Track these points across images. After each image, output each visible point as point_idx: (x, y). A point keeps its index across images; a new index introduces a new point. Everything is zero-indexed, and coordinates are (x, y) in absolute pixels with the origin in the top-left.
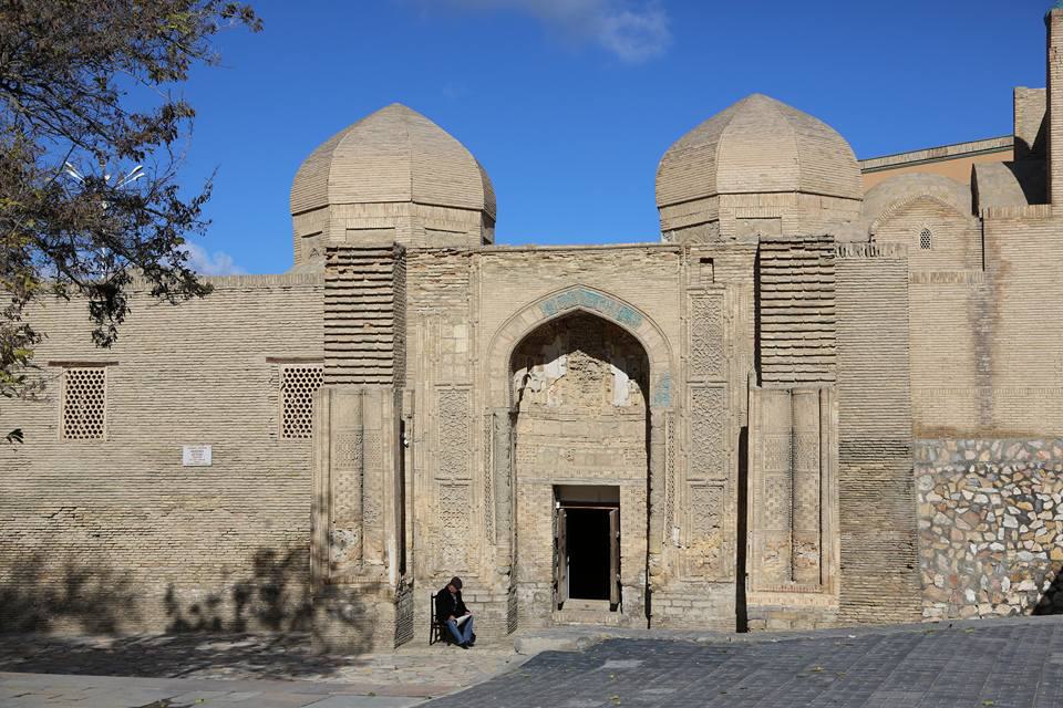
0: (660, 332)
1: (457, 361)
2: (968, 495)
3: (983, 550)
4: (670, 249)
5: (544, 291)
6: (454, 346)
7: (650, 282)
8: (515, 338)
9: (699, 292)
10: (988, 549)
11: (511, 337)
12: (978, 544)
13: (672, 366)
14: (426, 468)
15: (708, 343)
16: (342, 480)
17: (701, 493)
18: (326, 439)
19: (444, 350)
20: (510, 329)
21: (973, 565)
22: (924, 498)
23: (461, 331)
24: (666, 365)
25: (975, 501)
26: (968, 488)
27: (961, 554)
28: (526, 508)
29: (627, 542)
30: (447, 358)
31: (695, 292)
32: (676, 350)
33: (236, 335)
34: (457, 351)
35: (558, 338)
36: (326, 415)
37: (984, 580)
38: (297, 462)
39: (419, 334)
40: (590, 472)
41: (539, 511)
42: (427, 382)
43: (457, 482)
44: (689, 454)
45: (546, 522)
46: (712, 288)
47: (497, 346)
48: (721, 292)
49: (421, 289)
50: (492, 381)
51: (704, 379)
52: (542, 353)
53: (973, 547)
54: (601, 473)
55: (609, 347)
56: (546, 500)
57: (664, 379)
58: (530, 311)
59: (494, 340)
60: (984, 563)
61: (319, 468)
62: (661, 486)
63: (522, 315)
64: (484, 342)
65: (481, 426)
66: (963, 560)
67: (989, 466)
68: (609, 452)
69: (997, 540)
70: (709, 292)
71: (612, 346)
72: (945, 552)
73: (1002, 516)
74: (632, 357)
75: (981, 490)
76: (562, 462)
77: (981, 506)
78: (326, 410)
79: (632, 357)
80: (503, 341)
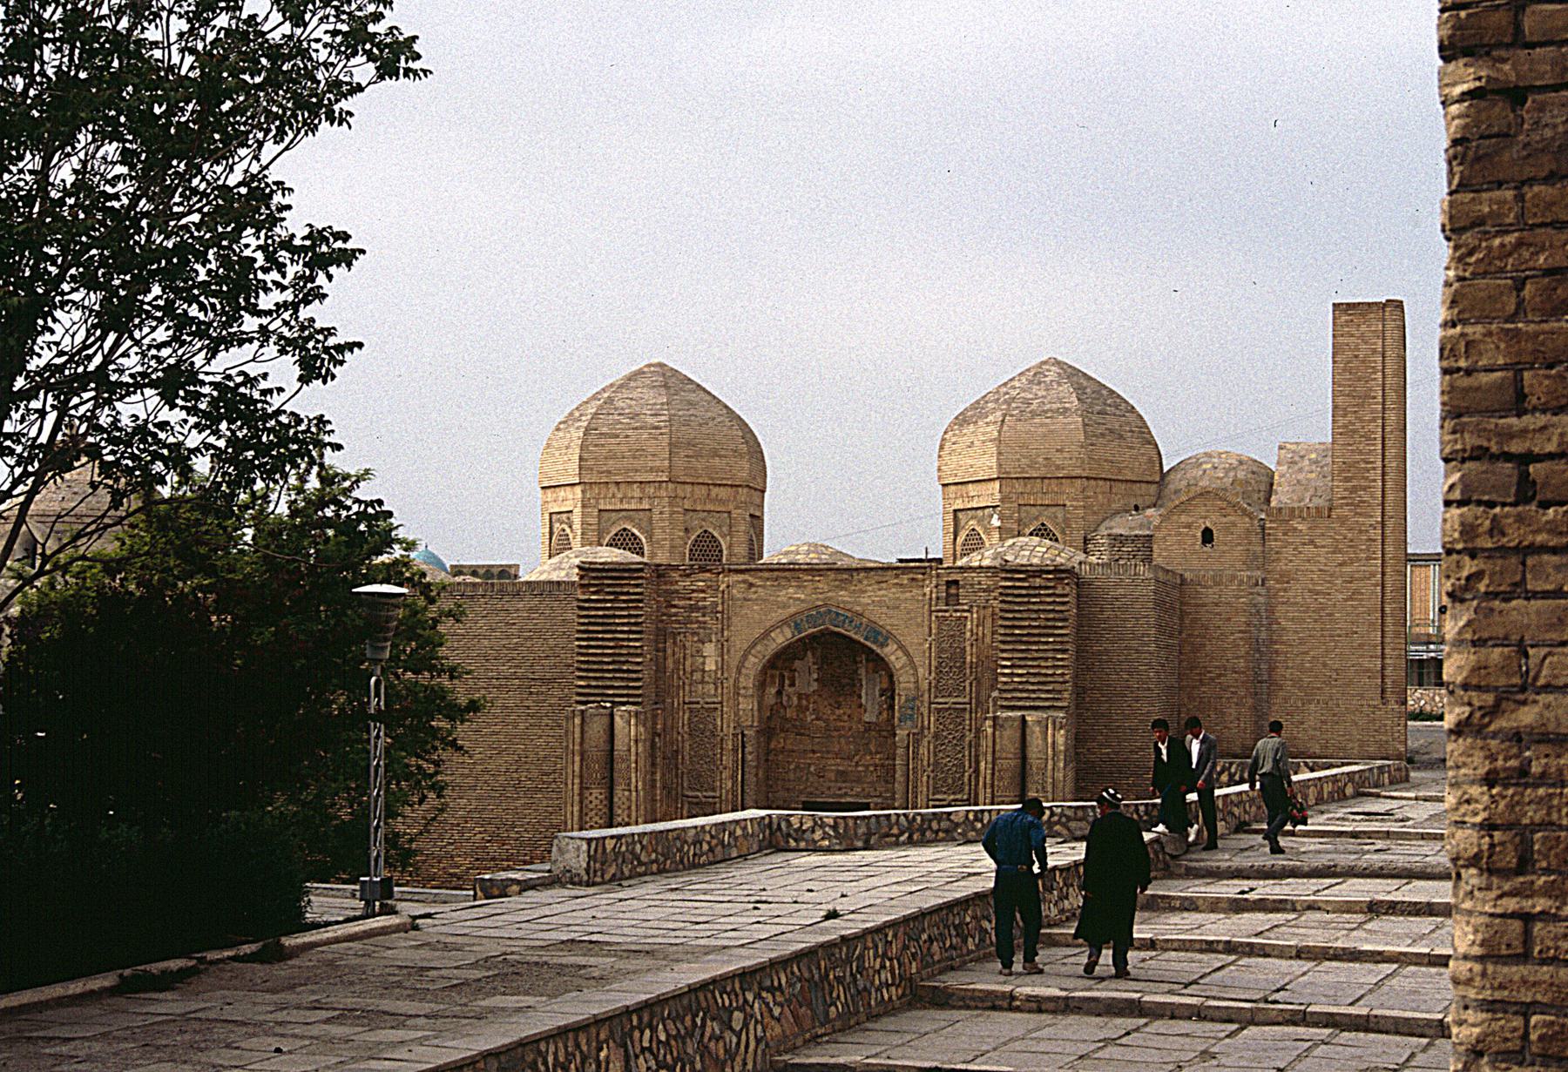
0: (907, 654)
5: (792, 610)
13: (917, 688)
15: (950, 661)
18: (577, 759)
20: (759, 648)
23: (709, 649)
33: (486, 642)
36: (577, 735)
38: (547, 774)
39: (669, 651)
59: (745, 657)
78: (577, 730)
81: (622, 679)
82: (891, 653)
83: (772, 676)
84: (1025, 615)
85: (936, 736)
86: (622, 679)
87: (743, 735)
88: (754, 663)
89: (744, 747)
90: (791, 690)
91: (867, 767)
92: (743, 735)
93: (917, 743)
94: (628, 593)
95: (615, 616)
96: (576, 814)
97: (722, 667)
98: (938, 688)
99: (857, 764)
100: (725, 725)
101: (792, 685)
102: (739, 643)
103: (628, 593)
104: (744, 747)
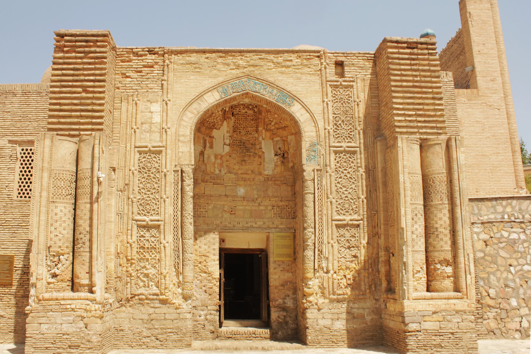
0: (308, 111)
1: (154, 129)
2: (506, 234)
3: (519, 271)
4: (314, 54)
5: (221, 79)
6: (152, 118)
7: (299, 75)
8: (198, 113)
9: (335, 83)
10: (521, 270)
11: (195, 112)
12: (515, 267)
13: (318, 136)
14: (126, 211)
16: (58, 211)
17: (342, 231)
19: (143, 121)
20: (195, 105)
21: (514, 281)
22: (478, 237)
23: (156, 107)
24: (314, 134)
25: (510, 237)
26: (505, 229)
27: (505, 275)
29: (275, 273)
30: (146, 127)
31: (332, 83)
32: (321, 124)
34: (153, 122)
37: (521, 291)
39: (124, 109)
43: (150, 223)
44: (334, 201)
47: (184, 118)
48: (351, 83)
50: (180, 144)
51: (342, 144)
53: (512, 268)
55: (262, 132)
56: (214, 244)
57: (313, 145)
58: (210, 93)
60: (521, 279)
61: (38, 198)
62: (313, 225)
63: (205, 96)
64: (173, 115)
65: (171, 178)
66: (506, 279)
67: (516, 215)
68: (262, 208)
69: (527, 264)
70: (343, 83)
71: (264, 131)
72: (494, 274)
73: (528, 247)
74: (278, 138)
75: (514, 230)
76: (227, 215)
77: (514, 242)
78: (47, 150)
80: (189, 114)
81: (87, 117)
82: (296, 111)
83: (199, 137)
84: (409, 73)
86: (87, 117)
87: (182, 172)
88: (191, 119)
89: (182, 181)
90: (211, 150)
91: (266, 206)
92: (182, 172)
93: (321, 177)
94: (95, 52)
95: (84, 69)
96: (42, 223)
99: (259, 205)
100: (169, 163)
101: (211, 147)
103: (95, 52)
104: (182, 181)
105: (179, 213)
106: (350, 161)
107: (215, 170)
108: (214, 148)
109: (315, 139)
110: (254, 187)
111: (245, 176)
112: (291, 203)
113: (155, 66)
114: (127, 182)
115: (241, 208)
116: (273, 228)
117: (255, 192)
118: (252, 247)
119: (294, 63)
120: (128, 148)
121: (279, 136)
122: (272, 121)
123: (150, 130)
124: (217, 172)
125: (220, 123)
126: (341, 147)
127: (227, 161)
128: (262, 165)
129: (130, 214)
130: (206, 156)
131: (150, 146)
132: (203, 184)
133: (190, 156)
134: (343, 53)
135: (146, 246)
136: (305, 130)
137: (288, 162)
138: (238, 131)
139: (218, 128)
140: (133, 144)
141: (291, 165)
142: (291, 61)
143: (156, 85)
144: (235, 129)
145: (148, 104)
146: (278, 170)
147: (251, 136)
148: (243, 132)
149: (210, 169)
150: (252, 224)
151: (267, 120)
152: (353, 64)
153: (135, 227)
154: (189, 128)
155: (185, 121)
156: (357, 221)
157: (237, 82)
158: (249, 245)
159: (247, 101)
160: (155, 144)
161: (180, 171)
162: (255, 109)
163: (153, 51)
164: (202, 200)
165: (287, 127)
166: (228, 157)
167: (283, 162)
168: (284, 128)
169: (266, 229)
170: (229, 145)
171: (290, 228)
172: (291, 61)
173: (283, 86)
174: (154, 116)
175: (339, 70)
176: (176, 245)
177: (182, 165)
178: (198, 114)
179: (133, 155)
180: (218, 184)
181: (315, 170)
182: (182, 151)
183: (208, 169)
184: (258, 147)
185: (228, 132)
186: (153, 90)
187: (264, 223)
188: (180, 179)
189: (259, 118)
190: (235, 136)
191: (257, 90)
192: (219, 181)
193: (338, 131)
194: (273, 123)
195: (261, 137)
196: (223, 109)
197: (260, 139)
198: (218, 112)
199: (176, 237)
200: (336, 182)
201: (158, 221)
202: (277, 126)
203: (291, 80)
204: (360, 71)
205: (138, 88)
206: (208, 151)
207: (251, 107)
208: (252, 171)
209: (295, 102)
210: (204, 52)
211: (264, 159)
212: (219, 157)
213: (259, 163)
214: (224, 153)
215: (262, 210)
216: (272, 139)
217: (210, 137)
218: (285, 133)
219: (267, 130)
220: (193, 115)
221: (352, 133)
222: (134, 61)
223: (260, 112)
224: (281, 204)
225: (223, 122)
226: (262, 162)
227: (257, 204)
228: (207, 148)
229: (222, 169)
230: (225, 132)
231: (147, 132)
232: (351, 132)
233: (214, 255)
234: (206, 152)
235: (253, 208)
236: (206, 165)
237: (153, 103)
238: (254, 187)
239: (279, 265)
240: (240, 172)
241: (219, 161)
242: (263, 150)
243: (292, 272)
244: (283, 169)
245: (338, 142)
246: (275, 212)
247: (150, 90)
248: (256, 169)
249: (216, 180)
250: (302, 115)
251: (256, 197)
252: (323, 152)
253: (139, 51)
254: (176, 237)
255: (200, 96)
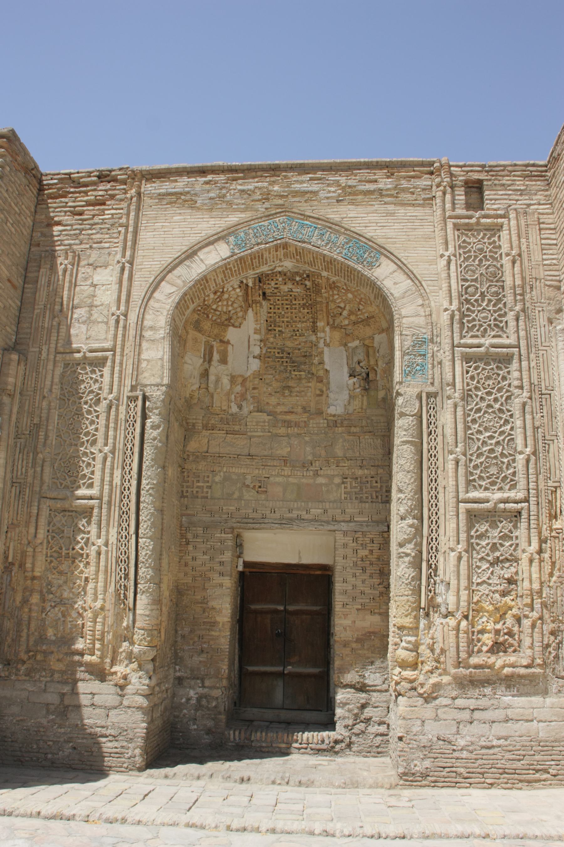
0: (411, 275)
1: (95, 316)
7: (391, 208)
11: (179, 282)
14: (30, 479)
20: (179, 271)
24: (421, 321)
28: (191, 563)
34: (95, 303)
35: (250, 313)
40: (290, 511)
41: (211, 569)
42: (45, 348)
45: (221, 585)
46: (485, 217)
48: (500, 220)
49: (59, 223)
51: (482, 341)
52: (226, 339)
54: (308, 512)
55: (324, 331)
68: (320, 480)
70: (483, 221)
71: (327, 329)
74: (357, 343)
76: (249, 495)
79: (357, 343)
80: (165, 287)
82: (385, 274)
83: (195, 340)
85: (467, 396)
89: (144, 417)
90: (222, 367)
97: (124, 296)
98: (463, 320)
99: (316, 474)
101: (224, 361)
102: (148, 264)
104: (144, 417)
105: (134, 483)
106: (498, 375)
107: (229, 407)
108: (230, 362)
109: (424, 331)
110: (307, 439)
111: (288, 417)
112: (380, 471)
113: (108, 203)
114: (36, 421)
115: (279, 479)
116: (344, 521)
117: (308, 449)
118: (305, 561)
119: (381, 186)
120: (44, 355)
121: (358, 338)
122: (344, 309)
123: (89, 318)
124: (234, 409)
125: (240, 314)
126: (479, 346)
127: (254, 389)
128: (324, 396)
129: (37, 482)
130: (212, 378)
131: (85, 348)
132: (205, 433)
133: (162, 366)
134: (483, 166)
135: (64, 552)
136: (404, 312)
137: (377, 390)
138: (277, 329)
139: (237, 324)
140: (53, 346)
141: (381, 394)
142: (376, 181)
143: (107, 236)
144: (271, 326)
145: (88, 271)
146: (356, 404)
147: (302, 339)
148: (287, 332)
149: (219, 402)
150: (300, 513)
151: (332, 306)
152: (503, 185)
153: (45, 512)
154: (165, 313)
155: (158, 301)
156: (516, 502)
157: (266, 223)
158: (300, 558)
159: (288, 265)
160: (96, 345)
161: (140, 398)
162: (307, 283)
163: (108, 175)
164: (202, 465)
165: (373, 317)
166: (257, 381)
167: (365, 389)
168: (367, 321)
169: (328, 523)
170: (259, 357)
171: (378, 522)
172: (376, 181)
173: (356, 230)
174: (98, 292)
175: (474, 197)
176: (123, 549)
177: (146, 386)
178: (184, 286)
179: (50, 366)
180: (234, 433)
181: (424, 395)
182: (147, 358)
183: (217, 403)
184: (316, 361)
185: (256, 332)
186: (103, 245)
187: (325, 511)
188: (139, 414)
189: (316, 302)
190: (272, 340)
191: (306, 238)
192: (237, 428)
193: (474, 315)
194: (345, 313)
195: (322, 341)
196: (242, 282)
197: (321, 344)
198: (234, 289)
199: (124, 533)
200: (469, 419)
201: (91, 498)
202: (353, 318)
203: (373, 217)
204: (517, 198)
205: (72, 242)
206: (216, 369)
207: (298, 279)
208: (304, 408)
209: (383, 259)
210: (203, 171)
211: (329, 383)
212: (240, 380)
213: (318, 392)
214: (249, 374)
215: (321, 485)
216: (345, 345)
217: (222, 341)
218: (368, 331)
219: (334, 327)
220: (174, 289)
221: (504, 319)
222: (70, 195)
223: (317, 288)
224: (360, 472)
225: (246, 312)
226: (324, 389)
227: (311, 473)
228: (215, 362)
229: (244, 404)
230: (251, 332)
231: (84, 323)
232: (500, 316)
233: (222, 574)
234: (212, 370)
235: (304, 481)
236: (212, 397)
237: (99, 270)
238: (307, 439)
239: (354, 599)
240: (279, 409)
241: (238, 388)
242: (327, 367)
243: (380, 614)
244: (365, 403)
245: (472, 337)
246: (349, 489)
247: (95, 245)
248: (312, 404)
249: (231, 424)
250: (395, 284)
251: (310, 458)
252: (440, 356)
253: (82, 177)
254: (124, 533)
255: (191, 254)
